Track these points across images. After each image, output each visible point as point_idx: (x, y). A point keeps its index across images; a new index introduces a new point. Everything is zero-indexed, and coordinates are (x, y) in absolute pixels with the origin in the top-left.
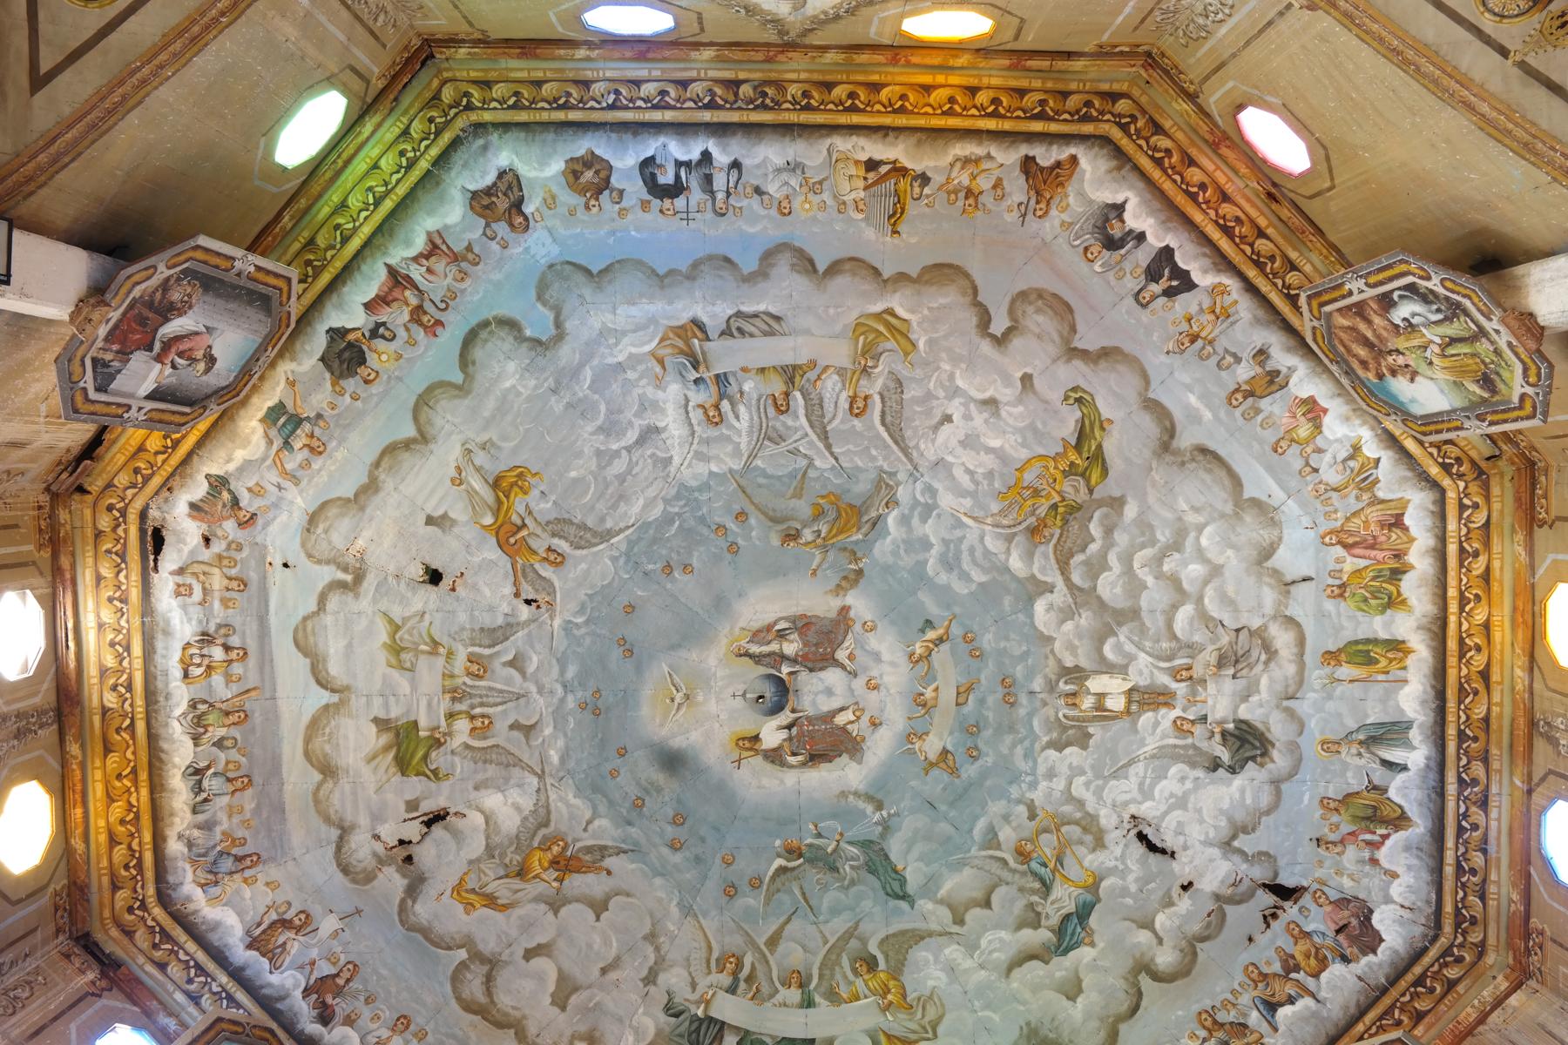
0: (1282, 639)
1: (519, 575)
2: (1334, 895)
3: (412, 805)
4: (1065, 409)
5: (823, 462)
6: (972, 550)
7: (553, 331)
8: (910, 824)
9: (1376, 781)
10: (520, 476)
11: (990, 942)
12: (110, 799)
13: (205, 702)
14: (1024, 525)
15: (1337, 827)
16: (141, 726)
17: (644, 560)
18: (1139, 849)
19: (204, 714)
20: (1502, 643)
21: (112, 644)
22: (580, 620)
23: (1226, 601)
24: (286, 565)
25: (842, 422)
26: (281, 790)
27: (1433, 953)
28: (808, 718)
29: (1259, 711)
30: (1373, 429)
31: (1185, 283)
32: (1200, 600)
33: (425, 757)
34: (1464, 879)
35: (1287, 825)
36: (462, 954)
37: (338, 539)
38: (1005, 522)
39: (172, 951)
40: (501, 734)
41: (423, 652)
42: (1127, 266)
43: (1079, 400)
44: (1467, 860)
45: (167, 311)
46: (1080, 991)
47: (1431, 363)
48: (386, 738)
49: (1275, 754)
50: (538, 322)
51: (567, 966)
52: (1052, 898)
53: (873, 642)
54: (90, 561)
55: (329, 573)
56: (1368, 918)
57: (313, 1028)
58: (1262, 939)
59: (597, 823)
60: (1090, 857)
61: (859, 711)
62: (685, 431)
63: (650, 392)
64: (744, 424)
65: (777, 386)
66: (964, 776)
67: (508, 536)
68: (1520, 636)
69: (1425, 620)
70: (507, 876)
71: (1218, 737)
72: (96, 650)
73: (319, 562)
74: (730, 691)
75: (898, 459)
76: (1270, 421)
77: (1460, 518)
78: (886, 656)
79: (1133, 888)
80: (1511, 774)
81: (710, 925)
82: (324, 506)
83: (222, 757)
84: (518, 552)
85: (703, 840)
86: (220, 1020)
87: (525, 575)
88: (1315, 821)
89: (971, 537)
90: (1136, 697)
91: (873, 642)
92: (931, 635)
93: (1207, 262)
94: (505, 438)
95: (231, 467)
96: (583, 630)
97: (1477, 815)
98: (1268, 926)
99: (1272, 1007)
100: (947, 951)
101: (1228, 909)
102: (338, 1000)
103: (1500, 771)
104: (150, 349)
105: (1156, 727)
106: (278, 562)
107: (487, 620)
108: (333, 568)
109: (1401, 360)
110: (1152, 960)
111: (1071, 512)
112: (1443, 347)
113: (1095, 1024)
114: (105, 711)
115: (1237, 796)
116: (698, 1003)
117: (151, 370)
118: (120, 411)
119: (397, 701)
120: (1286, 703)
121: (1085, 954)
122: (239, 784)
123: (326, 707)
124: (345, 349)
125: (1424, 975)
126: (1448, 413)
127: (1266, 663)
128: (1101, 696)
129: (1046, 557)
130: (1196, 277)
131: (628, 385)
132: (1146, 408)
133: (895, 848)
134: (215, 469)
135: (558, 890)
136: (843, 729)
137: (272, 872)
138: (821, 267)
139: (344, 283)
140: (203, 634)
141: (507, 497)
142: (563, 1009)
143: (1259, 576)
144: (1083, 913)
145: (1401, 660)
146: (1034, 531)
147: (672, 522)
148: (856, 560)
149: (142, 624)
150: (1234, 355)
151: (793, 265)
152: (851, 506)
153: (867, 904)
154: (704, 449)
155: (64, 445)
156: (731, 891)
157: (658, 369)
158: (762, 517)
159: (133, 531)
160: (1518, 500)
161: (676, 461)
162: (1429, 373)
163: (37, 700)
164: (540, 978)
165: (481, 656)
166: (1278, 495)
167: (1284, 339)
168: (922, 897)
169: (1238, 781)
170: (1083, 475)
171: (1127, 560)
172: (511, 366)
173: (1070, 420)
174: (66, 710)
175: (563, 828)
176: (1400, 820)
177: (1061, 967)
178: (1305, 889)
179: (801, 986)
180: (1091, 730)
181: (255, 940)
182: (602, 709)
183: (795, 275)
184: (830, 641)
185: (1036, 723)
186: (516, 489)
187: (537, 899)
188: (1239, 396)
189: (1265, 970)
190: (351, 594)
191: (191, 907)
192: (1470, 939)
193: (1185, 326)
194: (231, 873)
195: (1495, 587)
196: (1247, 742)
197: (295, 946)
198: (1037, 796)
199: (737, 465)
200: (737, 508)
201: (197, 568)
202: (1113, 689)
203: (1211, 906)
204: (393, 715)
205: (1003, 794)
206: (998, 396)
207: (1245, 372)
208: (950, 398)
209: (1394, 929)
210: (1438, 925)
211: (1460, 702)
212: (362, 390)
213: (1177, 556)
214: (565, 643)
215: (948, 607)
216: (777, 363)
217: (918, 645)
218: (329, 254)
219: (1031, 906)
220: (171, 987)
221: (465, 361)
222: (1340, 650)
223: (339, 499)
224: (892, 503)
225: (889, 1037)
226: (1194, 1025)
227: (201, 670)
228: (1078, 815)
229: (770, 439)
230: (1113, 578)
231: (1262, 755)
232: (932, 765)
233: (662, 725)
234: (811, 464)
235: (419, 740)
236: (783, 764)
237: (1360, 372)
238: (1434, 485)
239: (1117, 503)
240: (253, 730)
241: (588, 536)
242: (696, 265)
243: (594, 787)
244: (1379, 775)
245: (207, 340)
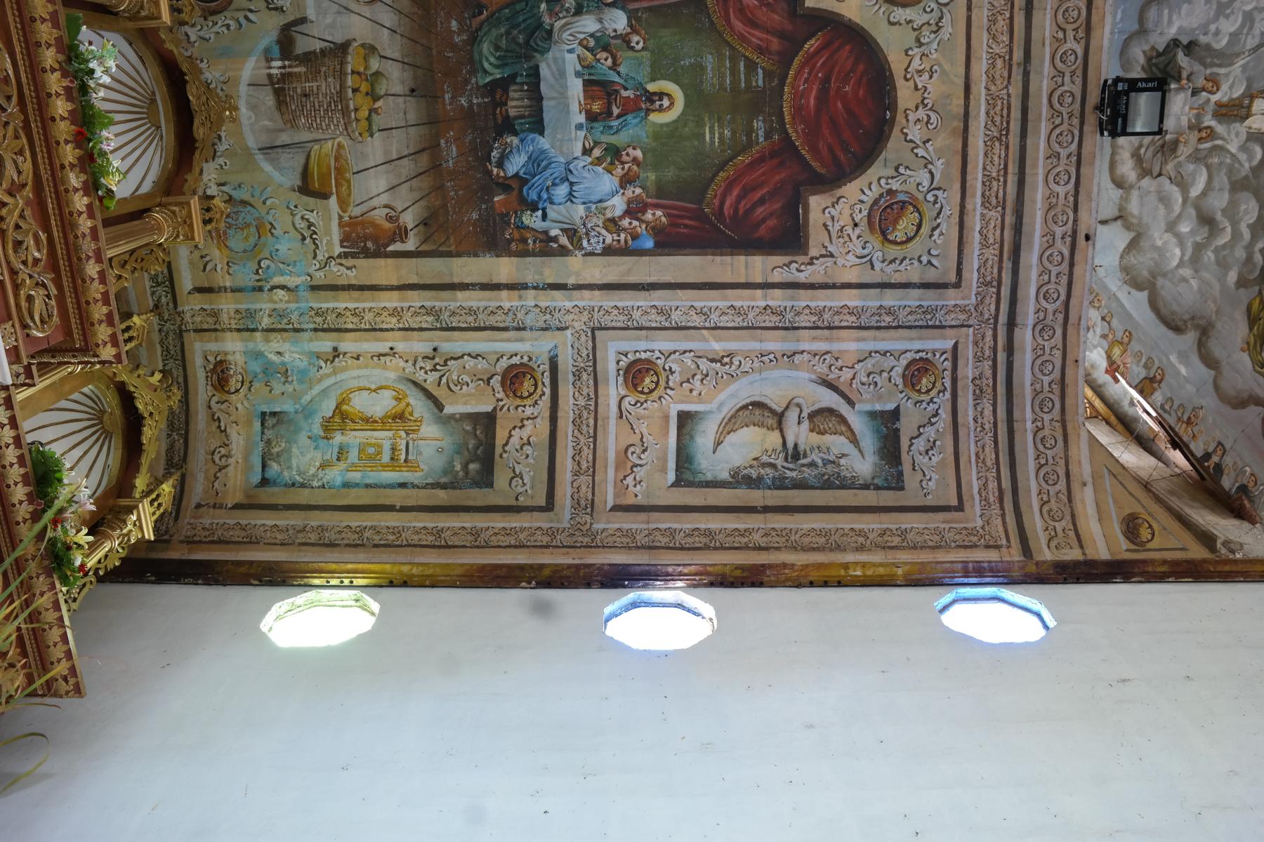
23: (1164, 200)
42: (1233, 474)
49: (1142, 60)
71: (1184, 75)
90: (1243, 112)
115: (1175, 17)
127: (1141, 146)
143: (1140, 224)
169: (1172, 31)
171: (1236, 235)
188: (1158, 377)
193: (1196, 429)
239: (1242, 283)
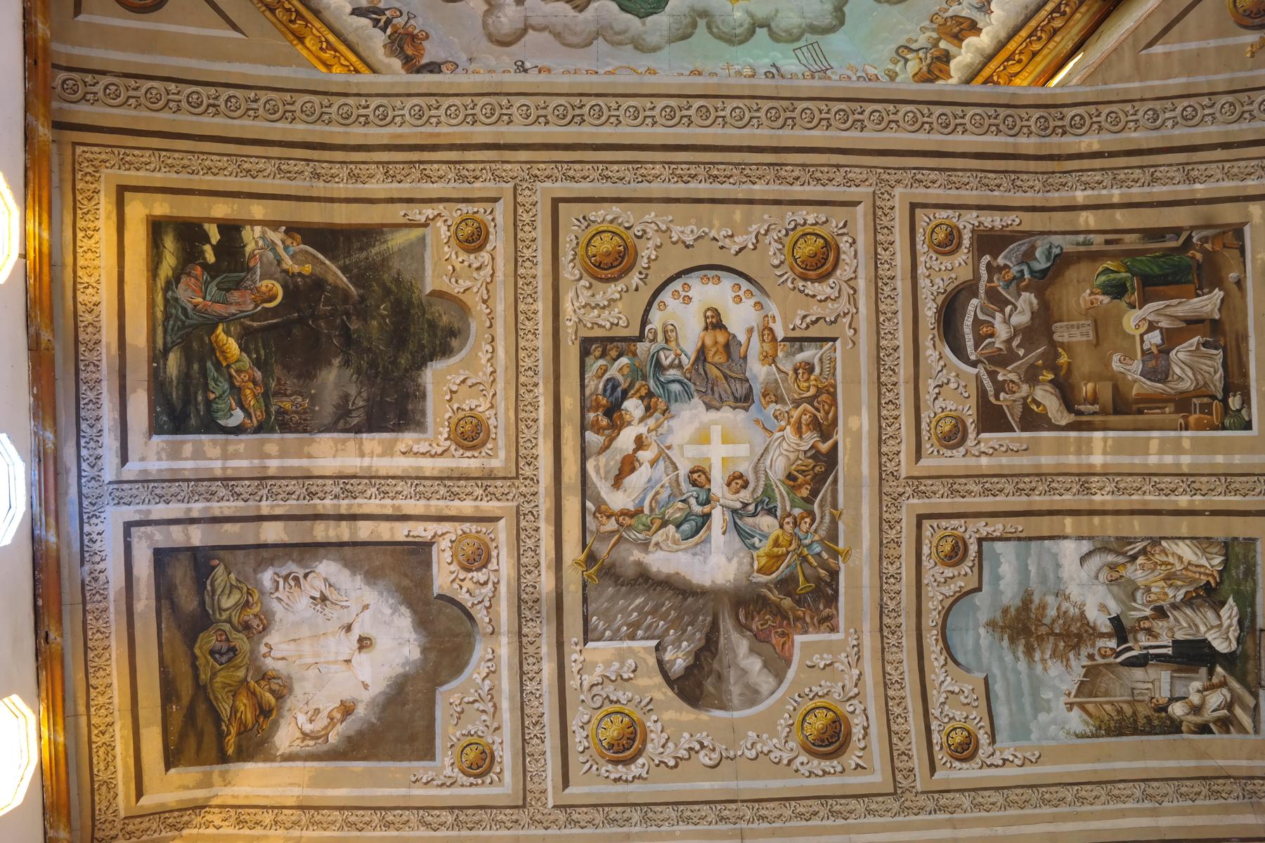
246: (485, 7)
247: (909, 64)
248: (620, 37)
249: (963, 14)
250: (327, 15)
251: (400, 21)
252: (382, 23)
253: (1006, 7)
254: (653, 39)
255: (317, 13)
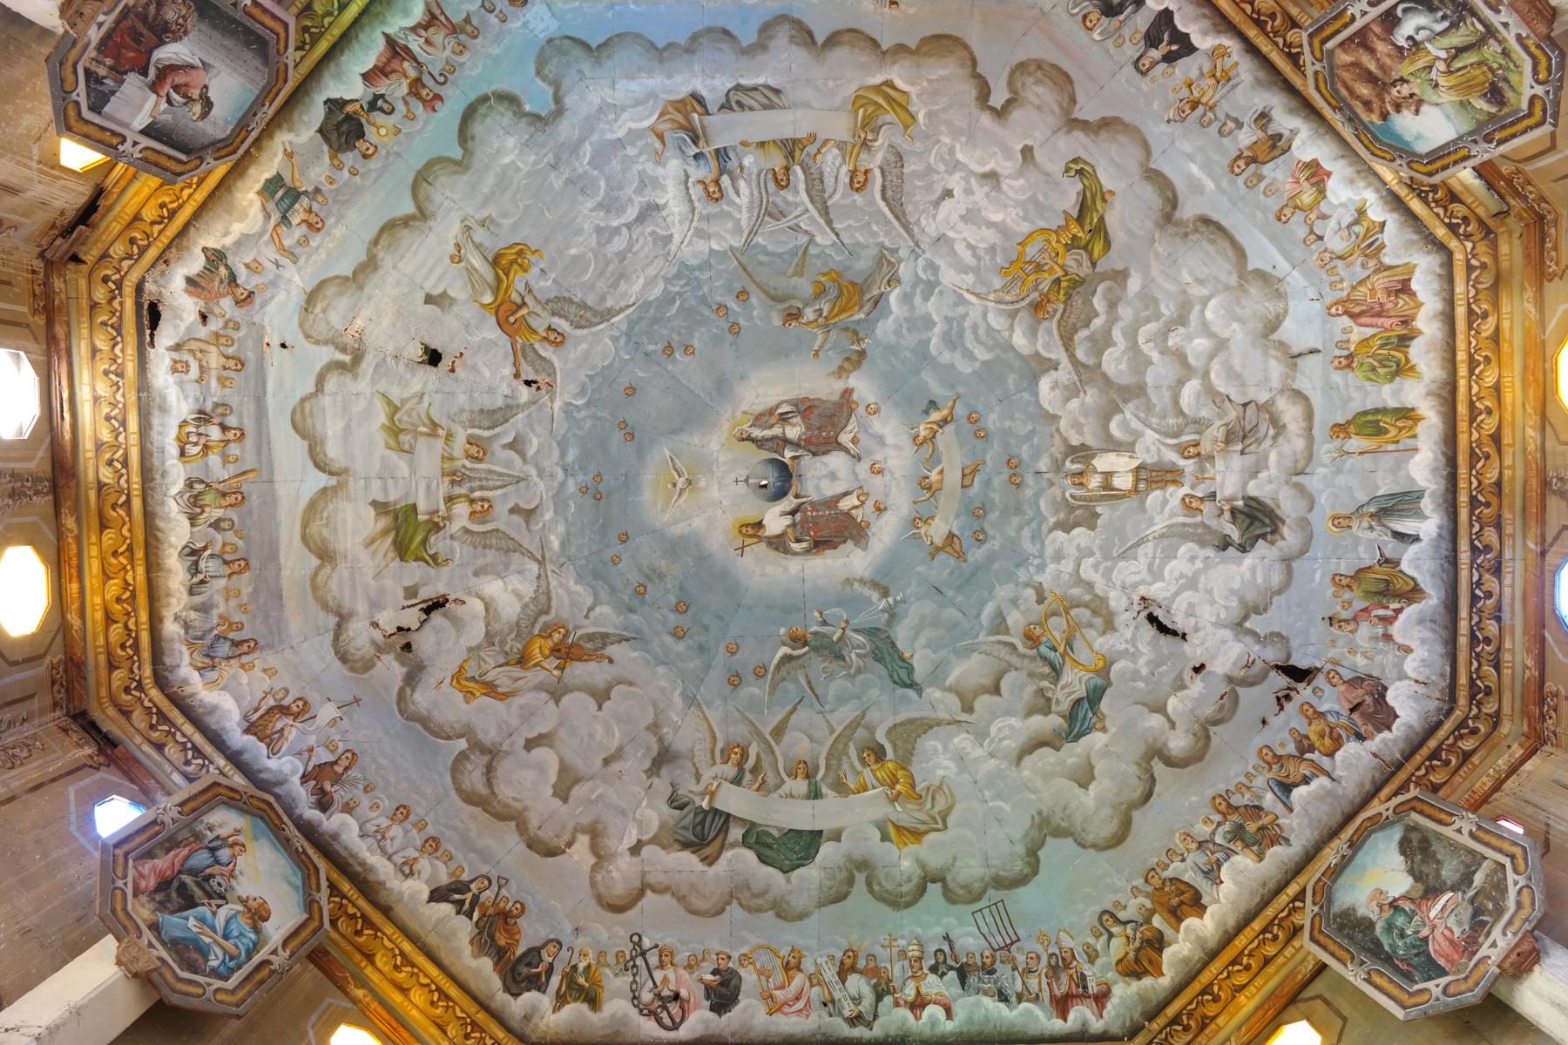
0: (1290, 413)
1: (520, 354)
2: (1347, 675)
3: (411, 592)
4: (1066, 180)
5: (824, 239)
6: (975, 327)
7: (553, 107)
8: (917, 610)
9: (1388, 555)
10: (520, 253)
11: (1000, 729)
12: (106, 577)
13: (202, 482)
14: (1027, 301)
15: (1350, 604)
16: (137, 504)
17: (645, 340)
18: (1149, 631)
19: (200, 494)
20: (1513, 405)
21: (108, 418)
22: (580, 402)
23: (1234, 376)
24: (283, 346)
25: (843, 196)
26: (278, 576)
27: (1448, 726)
28: (812, 504)
29: (1269, 488)
30: (1377, 191)
31: (1185, 47)
32: (1206, 374)
33: (424, 542)
34: (1478, 649)
35: (1299, 605)
36: (462, 744)
37: (336, 319)
38: (1008, 298)
39: (169, 732)
40: (501, 519)
41: (422, 434)
42: (1127, 32)
43: (1080, 172)
44: (1481, 629)
45: (163, 32)
46: (1092, 778)
47: (1437, 85)
48: (384, 522)
49: (1285, 530)
50: (537, 97)
51: (568, 756)
52: (1062, 682)
53: (877, 425)
54: (85, 332)
55: (327, 354)
56: (1382, 696)
57: (312, 814)
58: (1276, 722)
59: (598, 610)
60: (1101, 640)
61: (863, 495)
62: (686, 208)
63: (650, 168)
64: (744, 200)
65: (777, 161)
66: (971, 559)
67: (508, 314)
68: (1531, 394)
69: (1434, 386)
70: (507, 664)
71: (1227, 515)
72: (91, 424)
73: (317, 342)
74: (733, 476)
75: (899, 235)
76: (1273, 188)
77: (1468, 280)
78: (890, 440)
79: (1145, 671)
80: (1524, 537)
81: (714, 715)
82: (322, 284)
83: (219, 538)
84: (517, 332)
85: (706, 628)
86: (216, 784)
87: (525, 357)
88: (1327, 599)
89: (974, 314)
90: (1143, 475)
91: (877, 425)
92: (936, 416)
93: (1206, 23)
94: (505, 215)
95: (228, 241)
96: (583, 413)
97: (1490, 582)
98: (1282, 708)
99: (1286, 788)
100: (956, 740)
101: (1241, 691)
102: (336, 787)
103: (1513, 536)
104: (145, 74)
105: (1165, 505)
106: (276, 343)
107: (487, 402)
108: (331, 348)
109: (1405, 90)
110: (1165, 744)
111: (1075, 286)
112: (1449, 62)
113: (1106, 811)
114: (101, 486)
115: (1248, 575)
116: (703, 795)
117: (145, 100)
118: (115, 141)
119: (396, 485)
120: (1295, 479)
121: (1096, 740)
122: (235, 567)
123: (324, 490)
124: (343, 121)
125: (1439, 749)
126: (1454, 142)
127: (1275, 438)
128: (1108, 475)
129: (1049, 332)
130: (1196, 40)
131: (628, 162)
132: (1148, 178)
133: (901, 635)
134: (212, 242)
135: (559, 678)
136: (848, 515)
137: (271, 659)
138: (820, 39)
139: (342, 52)
140: (200, 412)
141: (507, 275)
142: (565, 800)
143: (1266, 349)
144: (1094, 697)
145: (1411, 428)
146: (1037, 307)
147: (673, 301)
148: (859, 341)
149: (138, 399)
150: (1236, 120)
151: (792, 37)
152: (853, 284)
153: (874, 693)
154: (704, 226)
155: (59, 204)
156: (735, 680)
157: (658, 145)
158: (763, 296)
159: (129, 304)
160: (1527, 256)
161: (677, 239)
162: (1435, 98)
163: (32, 466)
164: (542, 769)
165: (480, 438)
166: (1283, 266)
167: (1285, 101)
168: (930, 686)
169: (1249, 560)
170: (1085, 248)
171: (1131, 335)
172: (511, 142)
173: (1069, 196)
174: (62, 482)
175: (565, 615)
176: (1413, 593)
177: (1072, 753)
178: (1318, 670)
179: (807, 776)
180: (1099, 510)
181: (252, 724)
182: (604, 496)
183: (794, 48)
184: (834, 425)
185: (1042, 504)
186: (515, 267)
187: (539, 687)
188: (1241, 163)
189: (1280, 752)
190: (349, 375)
191: (188, 690)
192: (1485, 710)
194: (229, 658)
195: (1505, 347)
196: (1257, 520)
197: (293, 733)
198: (1046, 579)
199: (737, 242)
200: (738, 286)
201: (194, 345)
202: (1119, 467)
203: (1224, 688)
204: (391, 499)
205: (1010, 577)
206: (999, 170)
207: (1247, 137)
208: (950, 172)
209: (1408, 705)
210: (1453, 699)
211: (1472, 467)
212: (360, 165)
213: (1181, 330)
214: (566, 426)
215: (952, 387)
216: (778, 136)
217: (922, 427)
218: (327, 21)
219: (1041, 692)
220: (168, 768)
221: (464, 136)
222: (1349, 422)
223: (337, 277)
224: (894, 280)
225: (897, 827)
226: (1208, 810)
227: (199, 448)
228: (1087, 597)
229: (770, 215)
230: (1118, 354)
231: (1273, 532)
232: (938, 549)
233: (664, 511)
234: (812, 241)
235: (418, 524)
236: (787, 551)
237: (1364, 116)
238: (1441, 247)
239: (1121, 276)
240: (250, 513)
241: (589, 315)
242: (694, 38)
243: (596, 573)
244: (1391, 547)
245: (200, 78)
246: (593, 860)
247: (1114, 941)
248: (759, 901)
249: (1185, 879)
250: (400, 912)
251: (488, 895)
252: (467, 906)
253: (1240, 878)
254: (799, 902)
255: (386, 911)
